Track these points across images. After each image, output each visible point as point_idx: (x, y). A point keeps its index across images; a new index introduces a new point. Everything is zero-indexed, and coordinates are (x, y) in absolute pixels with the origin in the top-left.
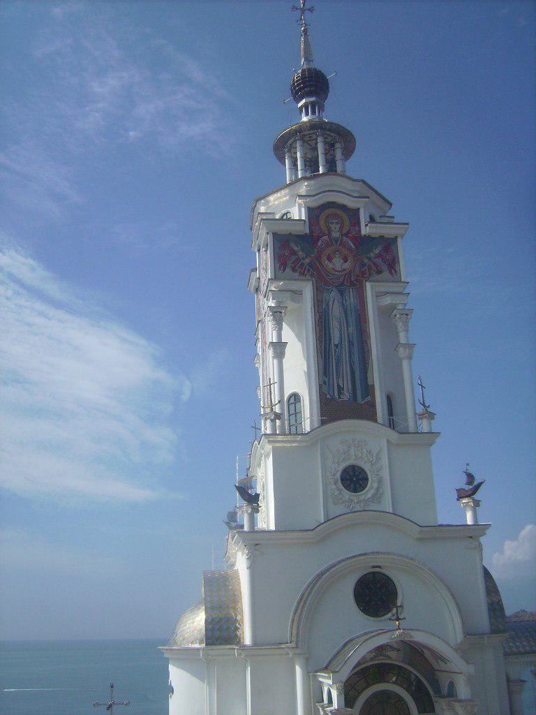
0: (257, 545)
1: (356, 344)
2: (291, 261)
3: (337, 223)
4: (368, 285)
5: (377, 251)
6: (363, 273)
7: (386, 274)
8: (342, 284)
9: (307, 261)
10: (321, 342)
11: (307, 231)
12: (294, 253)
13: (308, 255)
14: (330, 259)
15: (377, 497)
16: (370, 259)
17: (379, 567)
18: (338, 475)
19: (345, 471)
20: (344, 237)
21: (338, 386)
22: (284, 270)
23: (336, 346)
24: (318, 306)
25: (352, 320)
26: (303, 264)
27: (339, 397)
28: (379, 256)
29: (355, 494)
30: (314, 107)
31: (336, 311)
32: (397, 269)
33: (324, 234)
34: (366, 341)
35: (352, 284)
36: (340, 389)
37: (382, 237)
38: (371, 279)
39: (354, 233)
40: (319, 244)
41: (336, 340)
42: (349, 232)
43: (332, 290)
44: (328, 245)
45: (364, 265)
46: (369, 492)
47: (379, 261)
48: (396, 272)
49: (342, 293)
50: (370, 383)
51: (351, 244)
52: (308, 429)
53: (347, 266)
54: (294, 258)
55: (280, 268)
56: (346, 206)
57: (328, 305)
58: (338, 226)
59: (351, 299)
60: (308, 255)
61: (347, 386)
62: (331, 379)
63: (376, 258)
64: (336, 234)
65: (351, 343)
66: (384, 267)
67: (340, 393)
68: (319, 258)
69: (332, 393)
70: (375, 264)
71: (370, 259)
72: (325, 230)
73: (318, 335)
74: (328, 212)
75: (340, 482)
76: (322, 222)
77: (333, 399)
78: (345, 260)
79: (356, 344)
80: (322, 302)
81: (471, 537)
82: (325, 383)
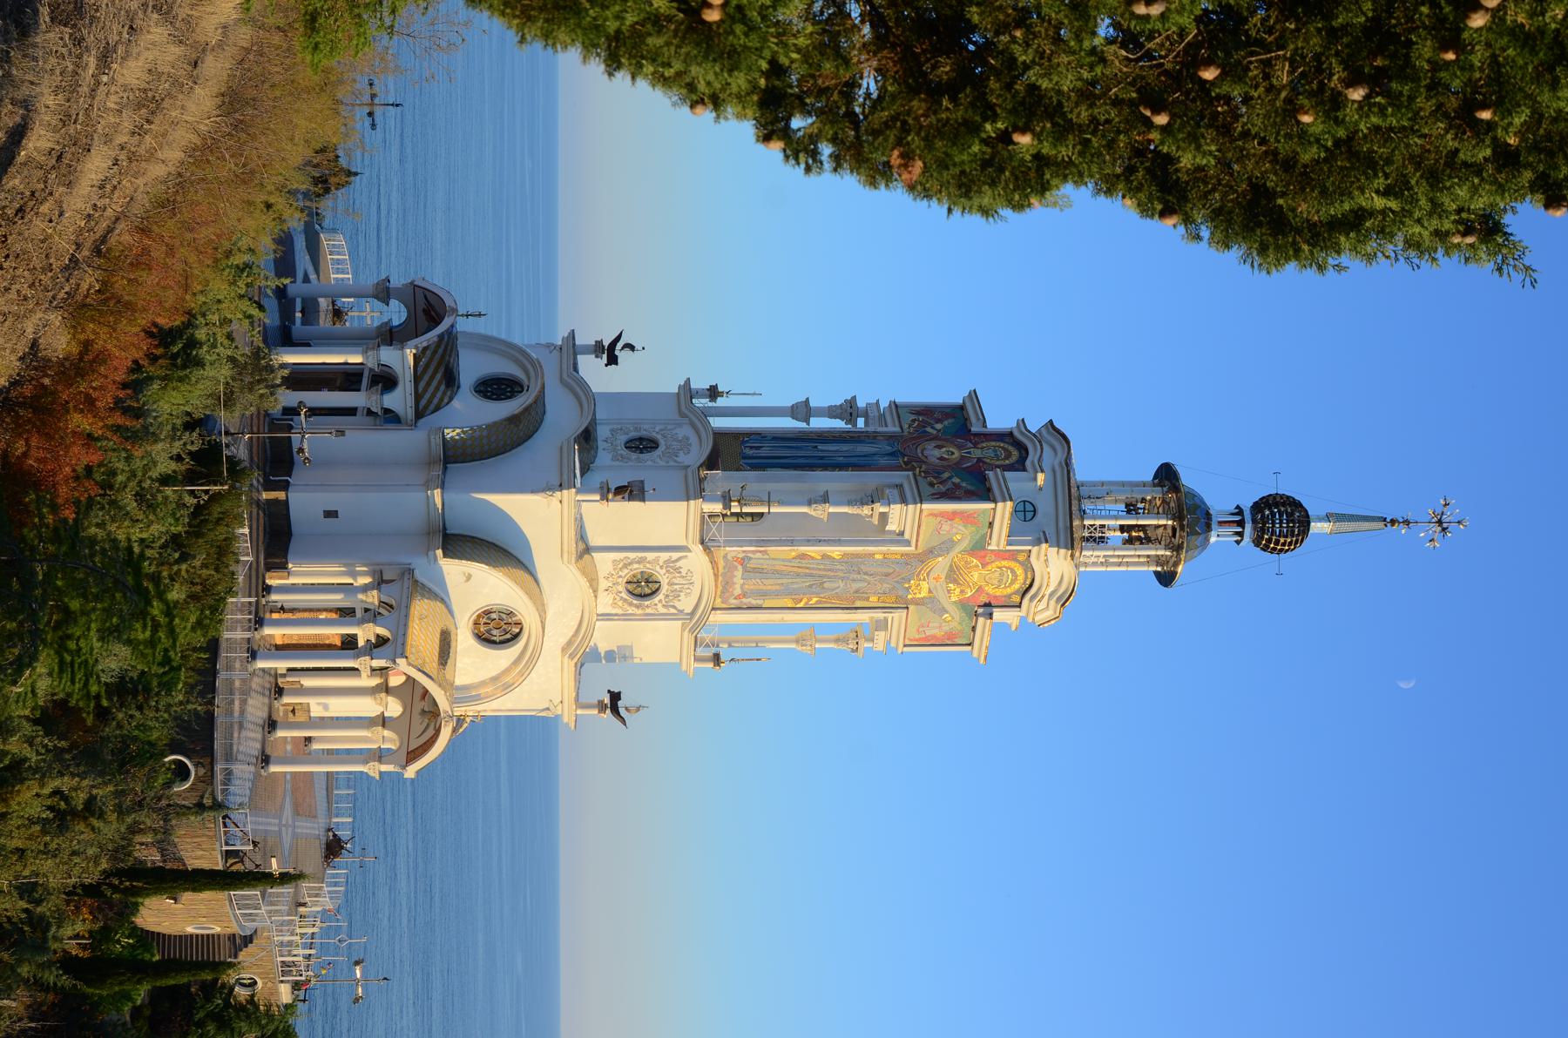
1: (820, 461)
5: (964, 485)
7: (932, 491)
9: (929, 429)
11: (974, 429)
12: (939, 421)
14: (939, 447)
16: (950, 478)
18: (643, 433)
30: (1237, 519)
36: (758, 448)
37: (989, 490)
42: (983, 462)
45: (939, 473)
46: (625, 452)
47: (949, 485)
49: (892, 454)
61: (762, 452)
65: (822, 458)
67: (751, 448)
68: (935, 438)
71: (950, 478)
77: (743, 442)
79: (820, 461)
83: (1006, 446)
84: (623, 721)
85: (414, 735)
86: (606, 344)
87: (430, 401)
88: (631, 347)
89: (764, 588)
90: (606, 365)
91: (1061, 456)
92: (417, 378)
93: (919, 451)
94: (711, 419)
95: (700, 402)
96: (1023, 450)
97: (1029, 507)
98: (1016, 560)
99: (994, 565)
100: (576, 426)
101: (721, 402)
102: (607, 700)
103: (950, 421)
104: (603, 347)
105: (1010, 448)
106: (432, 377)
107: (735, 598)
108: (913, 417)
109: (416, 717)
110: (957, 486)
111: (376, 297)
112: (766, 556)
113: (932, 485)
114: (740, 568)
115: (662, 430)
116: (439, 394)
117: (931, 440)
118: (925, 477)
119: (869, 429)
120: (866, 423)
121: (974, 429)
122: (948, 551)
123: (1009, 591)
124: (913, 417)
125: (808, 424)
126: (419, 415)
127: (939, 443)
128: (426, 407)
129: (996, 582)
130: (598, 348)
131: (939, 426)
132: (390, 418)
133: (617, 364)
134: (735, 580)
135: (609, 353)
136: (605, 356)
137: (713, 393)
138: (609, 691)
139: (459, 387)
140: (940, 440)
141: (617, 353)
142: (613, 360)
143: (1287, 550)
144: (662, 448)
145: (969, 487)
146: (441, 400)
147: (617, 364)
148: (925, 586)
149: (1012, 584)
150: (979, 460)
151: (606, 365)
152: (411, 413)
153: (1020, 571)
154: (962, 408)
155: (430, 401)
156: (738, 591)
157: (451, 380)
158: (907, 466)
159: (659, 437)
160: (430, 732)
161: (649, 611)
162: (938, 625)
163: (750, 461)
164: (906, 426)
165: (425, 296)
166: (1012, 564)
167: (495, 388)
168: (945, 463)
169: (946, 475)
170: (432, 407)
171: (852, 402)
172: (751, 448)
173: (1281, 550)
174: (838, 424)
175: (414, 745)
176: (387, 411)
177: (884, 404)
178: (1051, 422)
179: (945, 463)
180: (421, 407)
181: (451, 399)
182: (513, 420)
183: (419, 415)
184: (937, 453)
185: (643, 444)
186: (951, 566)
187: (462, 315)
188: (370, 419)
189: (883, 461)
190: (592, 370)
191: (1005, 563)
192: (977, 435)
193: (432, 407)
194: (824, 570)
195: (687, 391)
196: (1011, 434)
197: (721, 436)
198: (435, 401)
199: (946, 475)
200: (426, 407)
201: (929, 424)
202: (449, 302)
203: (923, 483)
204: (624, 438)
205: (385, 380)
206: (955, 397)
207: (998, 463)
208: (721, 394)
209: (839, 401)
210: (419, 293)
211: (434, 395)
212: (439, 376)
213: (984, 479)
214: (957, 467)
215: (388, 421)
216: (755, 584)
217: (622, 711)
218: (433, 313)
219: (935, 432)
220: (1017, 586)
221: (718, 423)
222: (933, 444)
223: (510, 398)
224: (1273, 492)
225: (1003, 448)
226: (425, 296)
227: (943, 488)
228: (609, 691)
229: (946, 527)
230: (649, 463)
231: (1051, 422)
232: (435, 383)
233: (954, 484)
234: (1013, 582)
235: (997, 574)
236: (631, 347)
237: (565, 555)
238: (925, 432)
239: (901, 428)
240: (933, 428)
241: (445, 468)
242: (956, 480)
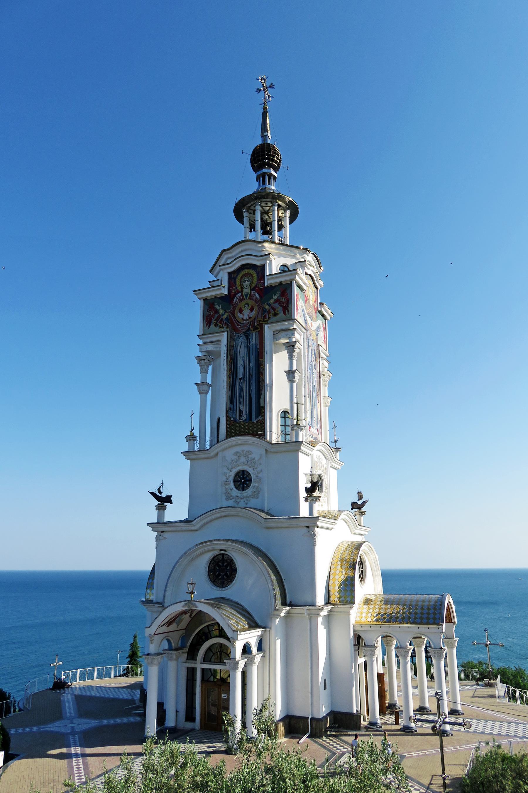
0: (162, 532)
1: (254, 376)
2: (215, 318)
3: (248, 281)
4: (266, 326)
5: (276, 297)
6: (264, 318)
7: (281, 315)
8: (248, 330)
9: (225, 316)
10: (230, 378)
11: (225, 291)
12: (216, 312)
13: (226, 312)
14: (241, 311)
15: (256, 495)
16: (270, 305)
17: (225, 550)
18: (231, 479)
19: (237, 474)
20: (252, 292)
21: (240, 410)
22: (209, 326)
23: (240, 379)
24: (230, 350)
26: (222, 319)
27: (240, 419)
28: (276, 301)
29: (243, 492)
31: (242, 352)
32: (289, 309)
33: (238, 292)
34: (262, 373)
35: (256, 328)
36: (241, 412)
37: (281, 283)
38: (269, 322)
39: (260, 286)
40: (234, 301)
41: (240, 375)
42: (256, 286)
43: (241, 336)
44: (241, 300)
46: (249, 491)
47: (276, 305)
48: (288, 311)
49: (247, 337)
50: (262, 405)
51: (257, 295)
52: (209, 447)
53: (253, 314)
54: (217, 315)
55: (207, 325)
56: (256, 265)
57: (237, 348)
58: (249, 283)
59: (254, 340)
60: (226, 312)
61: (245, 408)
62: (235, 406)
63: (274, 303)
65: (250, 376)
66: (279, 309)
67: (240, 416)
68: (233, 313)
69: (234, 416)
70: (274, 309)
71: (270, 305)
72: (240, 290)
73: (228, 373)
74: (242, 273)
75: (232, 483)
76: (238, 283)
78: (252, 310)
79: (254, 376)
80: (233, 347)
81: (308, 527)
82: (230, 409)
84: (365, 503)
86: (157, 503)
90: (171, 503)
99: (308, 294)
101: (196, 433)
117: (234, 316)
118: (269, 318)
121: (225, 291)
127: (237, 311)
130: (161, 508)
131: (221, 312)
133: (171, 496)
136: (165, 504)
141: (164, 495)
142: (168, 499)
143: (280, 157)
144: (246, 468)
145: (278, 294)
147: (171, 496)
151: (171, 503)
154: (205, 300)
161: (326, 482)
164: (222, 330)
169: (267, 307)
170: (250, 617)
171: (200, 360)
172: (240, 416)
173: (280, 161)
177: (201, 342)
189: (254, 340)
192: (230, 291)
199: (267, 307)
201: (219, 316)
209: (198, 366)
213: (271, 288)
225: (242, 278)
238: (226, 319)
239: (224, 331)
240: (223, 315)
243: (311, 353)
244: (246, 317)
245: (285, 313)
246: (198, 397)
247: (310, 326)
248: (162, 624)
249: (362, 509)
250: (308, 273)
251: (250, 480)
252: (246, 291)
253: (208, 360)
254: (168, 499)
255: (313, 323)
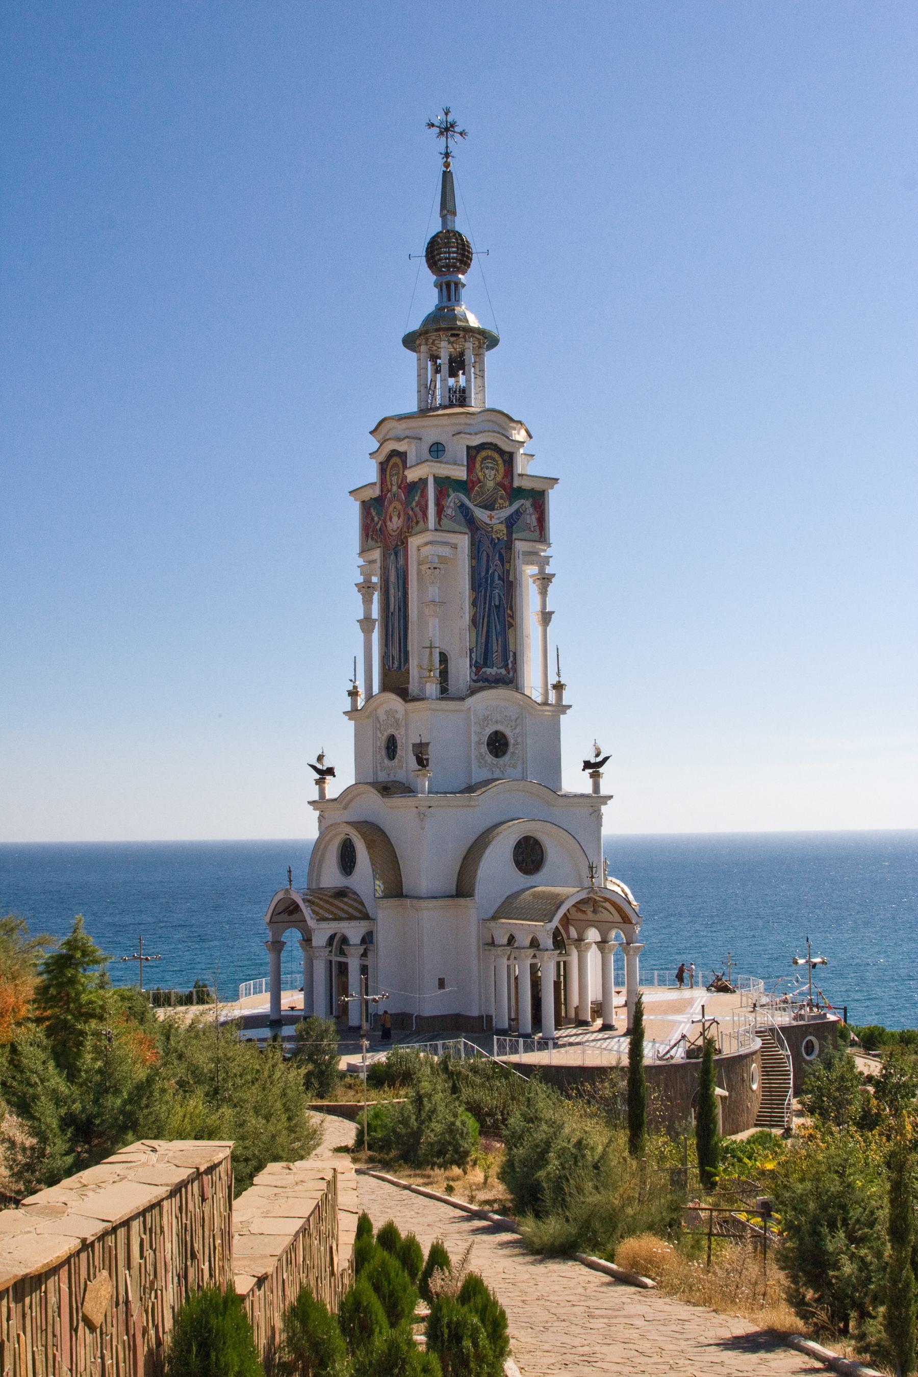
5: (417, 498)
8: (397, 545)
12: (372, 519)
14: (391, 520)
16: (412, 509)
25: (401, 582)
31: (393, 578)
37: (420, 479)
46: (396, 760)
47: (417, 509)
64: (395, 489)
65: (399, 609)
67: (393, 663)
68: (385, 522)
77: (389, 670)
78: (399, 517)
83: (389, 467)
84: (606, 759)
85: (610, 918)
86: (317, 776)
87: (356, 909)
88: (320, 758)
89: (499, 651)
90: (334, 776)
91: (393, 424)
92: (338, 919)
93: (394, 534)
94: (374, 694)
95: (361, 702)
96: (394, 453)
97: (434, 448)
98: (475, 457)
100: (373, 796)
102: (591, 771)
103: (372, 510)
104: (320, 778)
105: (391, 464)
106: (337, 907)
107: (509, 673)
108: (370, 539)
109: (599, 917)
110: (418, 504)
111: (279, 952)
112: (475, 649)
113: (417, 523)
114: (483, 670)
115: (381, 733)
116: (351, 902)
117: (386, 526)
119: (378, 572)
120: (375, 575)
121: (376, 492)
122: (467, 508)
123: (500, 462)
124: (370, 539)
125: (376, 620)
126: (366, 917)
128: (360, 911)
129: (493, 472)
130: (320, 782)
131: (376, 519)
132: (368, 939)
134: (494, 673)
135: (326, 773)
137: (353, 694)
138: (584, 770)
139: (347, 888)
140: (385, 519)
141: (325, 768)
142: (330, 771)
145: (419, 494)
146: (355, 900)
148: (496, 528)
149: (496, 461)
150: (399, 487)
151: (334, 776)
152: (364, 923)
153: (484, 453)
155: (356, 909)
156: (503, 671)
157: (341, 893)
158: (404, 543)
159: (385, 734)
160: (607, 905)
162: (528, 517)
163: (402, 664)
165: (279, 914)
166: (479, 459)
167: (347, 860)
168: (402, 513)
169: (411, 512)
170: (360, 907)
172: (393, 663)
174: (376, 597)
175: (617, 918)
176: (364, 941)
177: (361, 562)
178: (371, 433)
179: (402, 513)
180: (360, 916)
181: (355, 893)
182: (370, 846)
183: (366, 917)
184: (395, 519)
185: (391, 747)
186: (480, 507)
187: (290, 885)
188: (370, 954)
189: (401, 562)
190: (334, 788)
191: (478, 465)
192: (382, 491)
193: (360, 907)
194: (485, 604)
195: (353, 713)
196: (381, 463)
197: (385, 687)
198: (356, 905)
199: (411, 512)
200: (360, 911)
202: (281, 896)
203: (417, 529)
204: (386, 761)
205: (339, 943)
206: (354, 509)
207: (401, 472)
208: (355, 687)
209: (359, 597)
210: (276, 919)
211: (350, 906)
212: (336, 902)
214: (407, 504)
215: (371, 942)
216: (496, 656)
217: (599, 759)
218: (291, 908)
219: (380, 522)
220: (496, 456)
221: (376, 689)
222: (389, 523)
223: (354, 847)
224: (424, 259)
225: (391, 469)
226: (279, 914)
227: (420, 515)
228: (584, 770)
229: (449, 511)
230: (404, 741)
231: (371, 433)
232: (341, 905)
233: (417, 506)
234: (494, 459)
235: (487, 471)
236: (320, 758)
237: (472, 803)
240: (377, 524)
241: (406, 896)
242: (414, 504)
243: (488, 561)
244: (395, 528)
245: (424, 521)
246: (360, 636)
247: (487, 521)
248: (277, 911)
249: (601, 770)
250: (516, 419)
251: (396, 747)
252: (395, 489)
253: (369, 587)
254: (330, 771)
255: (493, 513)
